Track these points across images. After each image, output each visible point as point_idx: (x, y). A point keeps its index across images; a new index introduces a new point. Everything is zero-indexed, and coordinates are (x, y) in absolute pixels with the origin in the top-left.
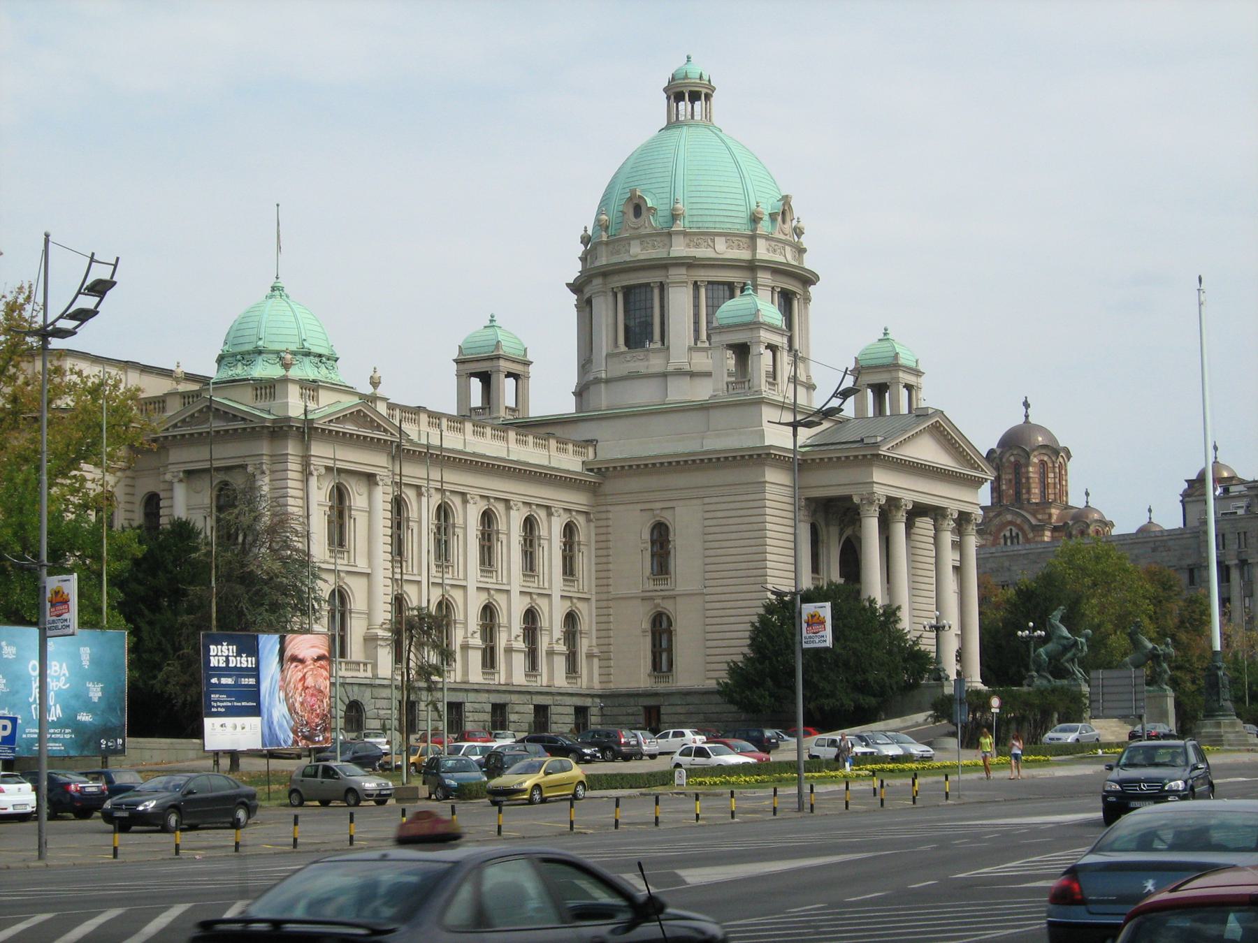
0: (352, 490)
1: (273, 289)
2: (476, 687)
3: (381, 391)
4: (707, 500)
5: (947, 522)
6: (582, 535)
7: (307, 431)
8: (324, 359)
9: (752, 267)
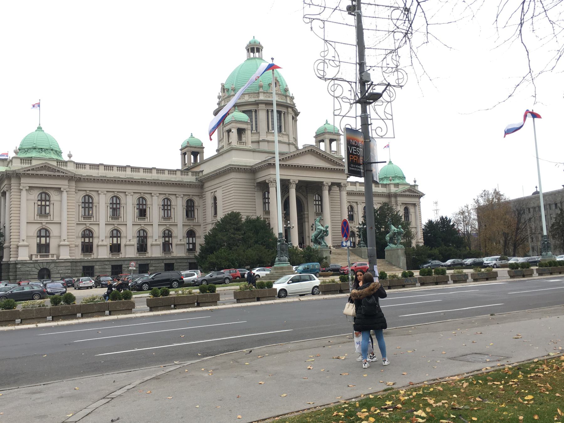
0: (52, 194)
1: (38, 128)
2: (128, 259)
3: (72, 159)
4: (222, 187)
5: (325, 187)
6: (196, 204)
7: (18, 175)
8: (43, 150)
9: (257, 103)
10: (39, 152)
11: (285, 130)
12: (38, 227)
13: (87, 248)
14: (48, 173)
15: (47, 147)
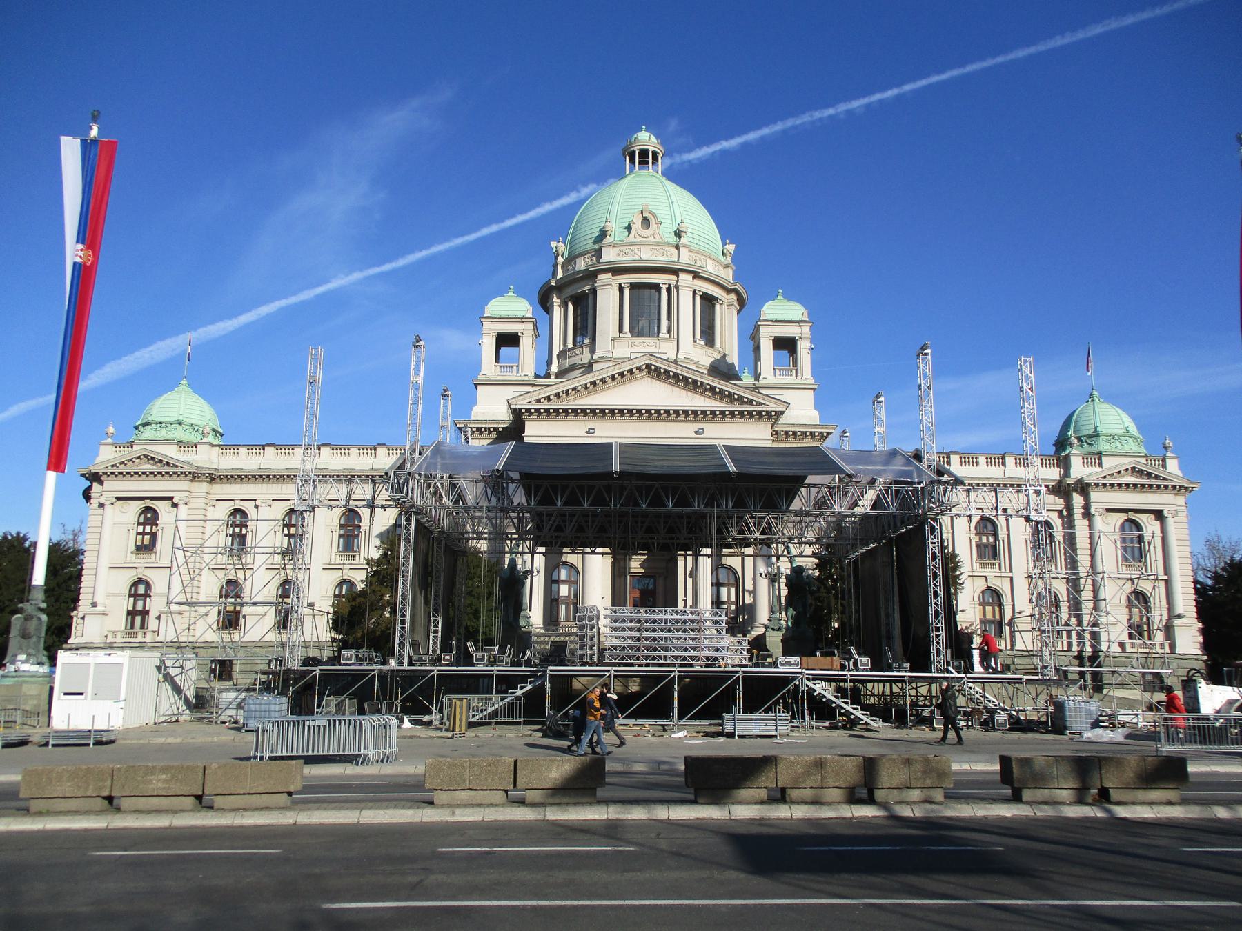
8: (163, 425)
9: (591, 275)
10: (156, 430)
11: (669, 331)
12: (131, 576)
13: (231, 621)
14: (148, 467)
15: (172, 420)
